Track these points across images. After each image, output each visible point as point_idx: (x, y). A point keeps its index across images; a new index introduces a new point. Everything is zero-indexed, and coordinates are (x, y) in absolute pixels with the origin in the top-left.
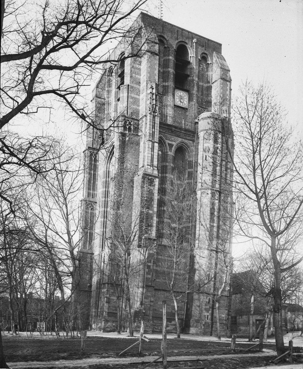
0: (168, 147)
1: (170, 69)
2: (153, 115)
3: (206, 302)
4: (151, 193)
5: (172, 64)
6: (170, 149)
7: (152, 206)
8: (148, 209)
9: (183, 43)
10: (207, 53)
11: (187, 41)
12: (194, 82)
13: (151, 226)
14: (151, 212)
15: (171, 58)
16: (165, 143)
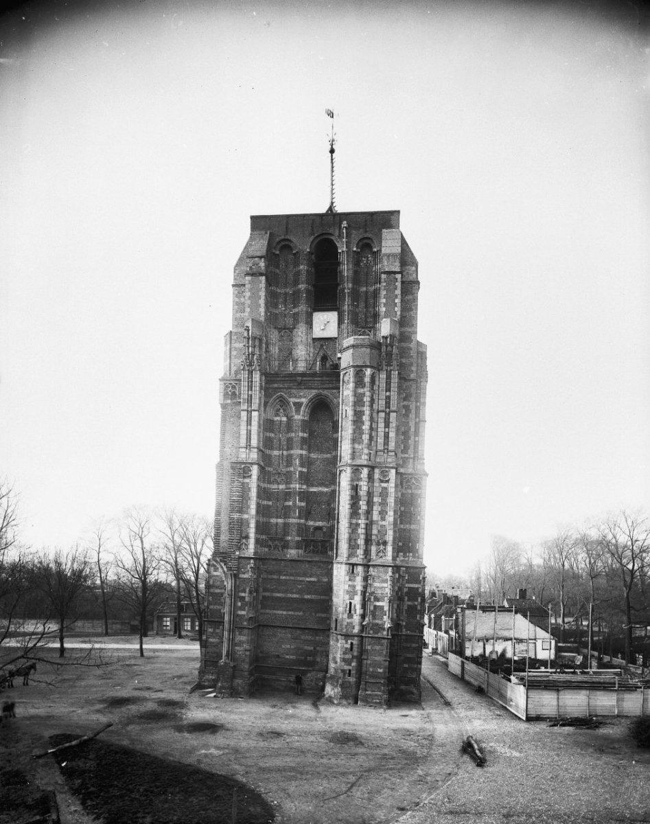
1: (300, 286)
3: (347, 648)
4: (245, 490)
5: (303, 277)
6: (298, 411)
7: (248, 507)
9: (326, 237)
11: (331, 231)
12: (346, 291)
13: (247, 537)
14: (246, 516)
15: (302, 267)
16: (288, 403)
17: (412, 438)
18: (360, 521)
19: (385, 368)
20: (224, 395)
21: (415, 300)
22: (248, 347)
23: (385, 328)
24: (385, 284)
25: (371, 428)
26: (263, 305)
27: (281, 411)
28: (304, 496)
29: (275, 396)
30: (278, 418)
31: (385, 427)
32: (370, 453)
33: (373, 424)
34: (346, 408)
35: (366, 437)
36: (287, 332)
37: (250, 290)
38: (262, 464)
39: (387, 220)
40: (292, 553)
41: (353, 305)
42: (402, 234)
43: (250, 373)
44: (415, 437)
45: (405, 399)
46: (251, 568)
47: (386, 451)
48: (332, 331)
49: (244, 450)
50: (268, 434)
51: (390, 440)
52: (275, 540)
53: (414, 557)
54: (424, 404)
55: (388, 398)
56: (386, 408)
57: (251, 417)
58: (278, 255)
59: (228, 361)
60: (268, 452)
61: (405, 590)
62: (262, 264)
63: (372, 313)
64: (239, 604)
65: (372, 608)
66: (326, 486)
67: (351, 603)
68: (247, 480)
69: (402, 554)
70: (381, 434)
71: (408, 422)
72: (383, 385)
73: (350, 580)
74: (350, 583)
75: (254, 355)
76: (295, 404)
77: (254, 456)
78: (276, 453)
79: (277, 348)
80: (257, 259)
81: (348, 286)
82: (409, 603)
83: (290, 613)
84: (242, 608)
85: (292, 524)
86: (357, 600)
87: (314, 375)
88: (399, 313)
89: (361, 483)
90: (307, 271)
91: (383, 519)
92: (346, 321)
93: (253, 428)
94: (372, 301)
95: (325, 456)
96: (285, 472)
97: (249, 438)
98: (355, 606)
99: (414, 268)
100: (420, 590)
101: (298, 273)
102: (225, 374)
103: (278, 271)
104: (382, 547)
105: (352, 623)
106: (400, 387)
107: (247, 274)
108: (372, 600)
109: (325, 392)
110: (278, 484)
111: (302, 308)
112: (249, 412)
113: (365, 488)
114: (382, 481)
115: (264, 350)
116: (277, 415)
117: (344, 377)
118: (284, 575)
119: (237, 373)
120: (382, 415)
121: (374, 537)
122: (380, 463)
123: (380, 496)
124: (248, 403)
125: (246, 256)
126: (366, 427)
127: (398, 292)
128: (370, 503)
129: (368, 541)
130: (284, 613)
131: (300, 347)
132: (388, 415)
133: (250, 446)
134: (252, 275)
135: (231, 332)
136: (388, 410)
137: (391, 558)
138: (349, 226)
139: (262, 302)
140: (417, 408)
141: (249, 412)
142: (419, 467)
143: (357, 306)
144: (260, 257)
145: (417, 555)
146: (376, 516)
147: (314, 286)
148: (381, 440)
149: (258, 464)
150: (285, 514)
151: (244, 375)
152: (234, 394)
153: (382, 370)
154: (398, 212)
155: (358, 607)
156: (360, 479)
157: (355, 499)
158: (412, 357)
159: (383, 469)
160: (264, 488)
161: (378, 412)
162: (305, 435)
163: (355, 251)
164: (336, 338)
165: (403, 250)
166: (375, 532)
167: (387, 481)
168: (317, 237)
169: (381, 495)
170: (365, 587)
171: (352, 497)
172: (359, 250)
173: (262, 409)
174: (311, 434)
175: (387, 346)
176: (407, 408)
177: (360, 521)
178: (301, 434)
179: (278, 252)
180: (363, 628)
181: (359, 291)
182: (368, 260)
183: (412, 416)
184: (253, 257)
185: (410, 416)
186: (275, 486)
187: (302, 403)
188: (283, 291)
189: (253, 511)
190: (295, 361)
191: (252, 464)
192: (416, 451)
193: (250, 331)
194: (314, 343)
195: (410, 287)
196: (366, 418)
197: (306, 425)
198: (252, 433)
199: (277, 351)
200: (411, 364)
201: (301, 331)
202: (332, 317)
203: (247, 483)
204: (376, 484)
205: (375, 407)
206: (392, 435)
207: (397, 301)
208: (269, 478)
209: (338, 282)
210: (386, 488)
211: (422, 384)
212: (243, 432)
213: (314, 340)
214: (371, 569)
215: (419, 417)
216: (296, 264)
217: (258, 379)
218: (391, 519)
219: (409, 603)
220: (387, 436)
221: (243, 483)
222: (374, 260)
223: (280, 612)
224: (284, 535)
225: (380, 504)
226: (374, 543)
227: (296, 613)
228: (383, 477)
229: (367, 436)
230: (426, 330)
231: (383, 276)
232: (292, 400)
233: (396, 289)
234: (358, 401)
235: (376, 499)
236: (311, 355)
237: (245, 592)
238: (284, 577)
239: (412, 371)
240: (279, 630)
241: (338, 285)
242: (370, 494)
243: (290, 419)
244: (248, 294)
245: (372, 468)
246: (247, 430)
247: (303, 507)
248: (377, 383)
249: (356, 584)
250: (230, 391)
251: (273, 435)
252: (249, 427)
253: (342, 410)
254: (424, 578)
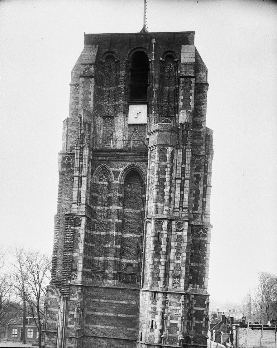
0: (113, 175)
1: (120, 86)
2: (80, 147)
4: (75, 234)
5: (122, 79)
6: (116, 178)
7: (78, 248)
8: (71, 252)
10: (172, 50)
11: (143, 46)
12: (154, 90)
13: (76, 270)
14: (75, 255)
15: (121, 72)
17: (201, 199)
18: (161, 260)
19: (182, 146)
20: (62, 165)
21: (205, 97)
22: (81, 130)
23: (183, 117)
24: (182, 85)
25: (171, 192)
26: (92, 99)
27: (104, 177)
28: (120, 240)
29: (99, 166)
30: (101, 183)
31: (181, 191)
32: (169, 210)
33: (172, 188)
34: (152, 176)
35: (166, 198)
36: (110, 118)
37: (83, 88)
38: (89, 216)
39: (185, 38)
40: (110, 283)
41: (158, 100)
42: (196, 50)
43: (82, 149)
44: (203, 198)
45: (196, 170)
46: (79, 293)
47: (181, 208)
48: (142, 119)
49: (76, 205)
50: (94, 194)
51: (184, 200)
52: (97, 273)
53: (200, 287)
54: (210, 173)
55: (183, 169)
56: (182, 177)
57: (81, 181)
58: (104, 62)
59: (66, 140)
60: (93, 207)
61: (194, 312)
62: (92, 69)
63: (173, 106)
64: (69, 320)
65: (168, 325)
66: (136, 233)
67: (152, 321)
68: (77, 228)
69: (191, 285)
70: (178, 196)
71: (198, 187)
72: (180, 159)
73: (152, 304)
74: (153, 306)
75: (84, 136)
76: (114, 172)
77: (83, 210)
78: (99, 208)
79: (101, 131)
80: (88, 66)
81: (155, 86)
82: (197, 322)
83: (107, 327)
84: (71, 323)
85: (110, 261)
86: (158, 319)
87: (129, 151)
88: (192, 107)
89: (163, 232)
90: (125, 75)
91: (178, 259)
92: (153, 112)
93: (82, 189)
94: (172, 97)
95: (136, 211)
96: (105, 223)
97: (79, 197)
98: (156, 323)
99: (204, 74)
100: (205, 312)
101: (119, 76)
102: (63, 149)
103: (103, 74)
104: (177, 280)
105: (153, 336)
106: (192, 161)
107: (81, 77)
108: (169, 318)
109: (137, 164)
110: (101, 231)
111: (121, 102)
112: (80, 178)
113: (165, 236)
114: (178, 231)
115: (92, 132)
116: (101, 180)
117: (151, 153)
118: (104, 299)
119: (72, 148)
120: (179, 181)
121: (171, 272)
122: (176, 217)
123: (176, 242)
124: (79, 171)
125: (81, 64)
126: (167, 190)
127: (192, 91)
128: (168, 247)
129: (166, 275)
130: (103, 327)
131: (119, 130)
132: (183, 182)
133: (80, 202)
134: (85, 77)
135: (68, 119)
136: (183, 178)
137: (183, 288)
138: (157, 42)
139: (91, 97)
140: (205, 178)
141: (80, 178)
142: (206, 220)
143: (162, 101)
144: (91, 64)
145: (203, 286)
146: (172, 256)
147: (130, 86)
148: (177, 200)
149: (86, 216)
150: (105, 253)
151: (77, 150)
152: (69, 164)
153: (179, 148)
154: (194, 32)
155: (158, 324)
156: (162, 229)
157: (157, 243)
158: (202, 138)
159: (179, 222)
160: (90, 234)
161: (176, 179)
162: (121, 195)
163: (161, 61)
164: (146, 124)
165: (197, 60)
166: (172, 268)
167: (182, 231)
168: (133, 50)
169: (177, 241)
170: (164, 309)
171: (155, 242)
172: (164, 60)
173: (90, 175)
174: (126, 194)
175: (183, 131)
176: (198, 177)
177: (161, 260)
178: (118, 195)
179: (104, 61)
180: (161, 339)
181: (163, 90)
182: (170, 67)
183: (201, 183)
184: (85, 64)
185: (200, 182)
186: (98, 233)
187: (119, 172)
188: (107, 89)
189: (81, 251)
190: (115, 141)
191: (81, 216)
192: (204, 208)
193: (82, 119)
194: (129, 127)
195: (201, 88)
196: (167, 184)
197: (122, 188)
198: (82, 193)
199: (102, 132)
200: (201, 145)
201: (119, 120)
202: (143, 108)
203: (78, 230)
204: (173, 233)
206: (186, 196)
207: (191, 97)
208: (94, 227)
209: (148, 83)
210: (180, 236)
211: (209, 159)
212: (75, 192)
213: (130, 125)
214: (168, 296)
215: (206, 184)
216: (117, 69)
217: (87, 154)
218: (184, 259)
219: (197, 322)
220: (182, 197)
221: (74, 230)
222: (175, 67)
223: (99, 326)
224: (104, 269)
225: (176, 247)
226: (171, 277)
227: (112, 328)
228: (179, 227)
229: (168, 197)
230: (212, 120)
231: (182, 79)
232: (112, 169)
233: (191, 89)
234: (162, 171)
235: (173, 244)
236: (127, 136)
237: (74, 311)
238: (103, 301)
239: (202, 149)
240: (99, 340)
241: (148, 85)
242: (169, 240)
243: (110, 183)
244: (81, 91)
245: (170, 221)
246: (78, 191)
247: (118, 248)
248: (175, 158)
249: (156, 306)
250: (66, 162)
251: (97, 195)
252: (79, 188)
253: (149, 177)
254: (208, 304)
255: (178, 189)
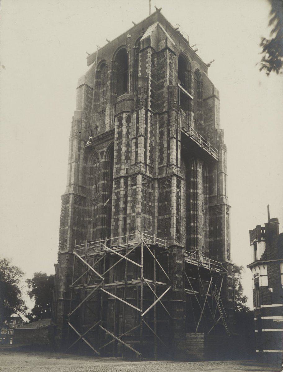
114: (132, 185)
123: (132, 196)
129: (125, 230)
159: (133, 177)
205: (130, 137)
210: (135, 189)
225: (132, 201)
235: (129, 199)
255: (134, 147)
